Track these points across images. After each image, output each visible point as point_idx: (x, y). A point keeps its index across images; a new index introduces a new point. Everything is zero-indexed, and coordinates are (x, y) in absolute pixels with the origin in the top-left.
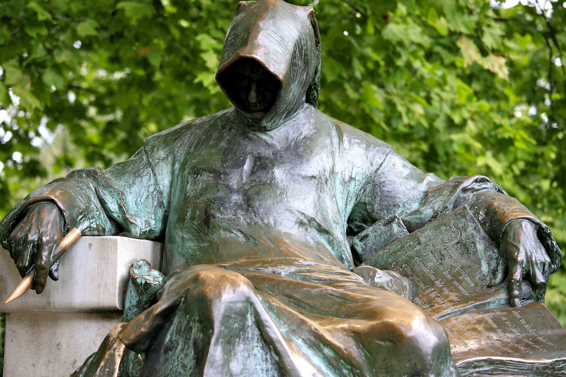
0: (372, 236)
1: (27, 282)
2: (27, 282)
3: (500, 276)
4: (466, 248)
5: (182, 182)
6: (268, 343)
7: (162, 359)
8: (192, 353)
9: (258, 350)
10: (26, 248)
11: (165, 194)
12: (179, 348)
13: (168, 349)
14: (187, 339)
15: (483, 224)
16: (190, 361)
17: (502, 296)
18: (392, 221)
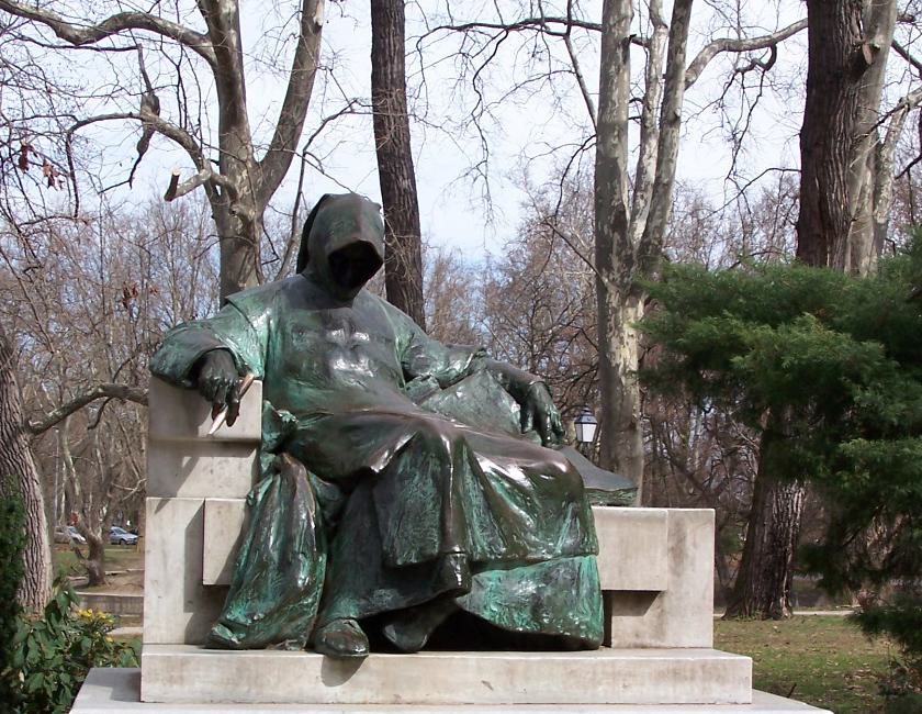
0: (413, 389)
1: (222, 416)
2: (222, 416)
3: (530, 425)
4: (495, 401)
5: (283, 338)
6: (477, 473)
7: (398, 486)
8: (430, 481)
9: (469, 480)
10: (224, 387)
11: (265, 345)
12: (417, 477)
13: (402, 479)
14: (424, 472)
15: (504, 385)
16: (430, 488)
17: (538, 439)
18: (428, 377)
